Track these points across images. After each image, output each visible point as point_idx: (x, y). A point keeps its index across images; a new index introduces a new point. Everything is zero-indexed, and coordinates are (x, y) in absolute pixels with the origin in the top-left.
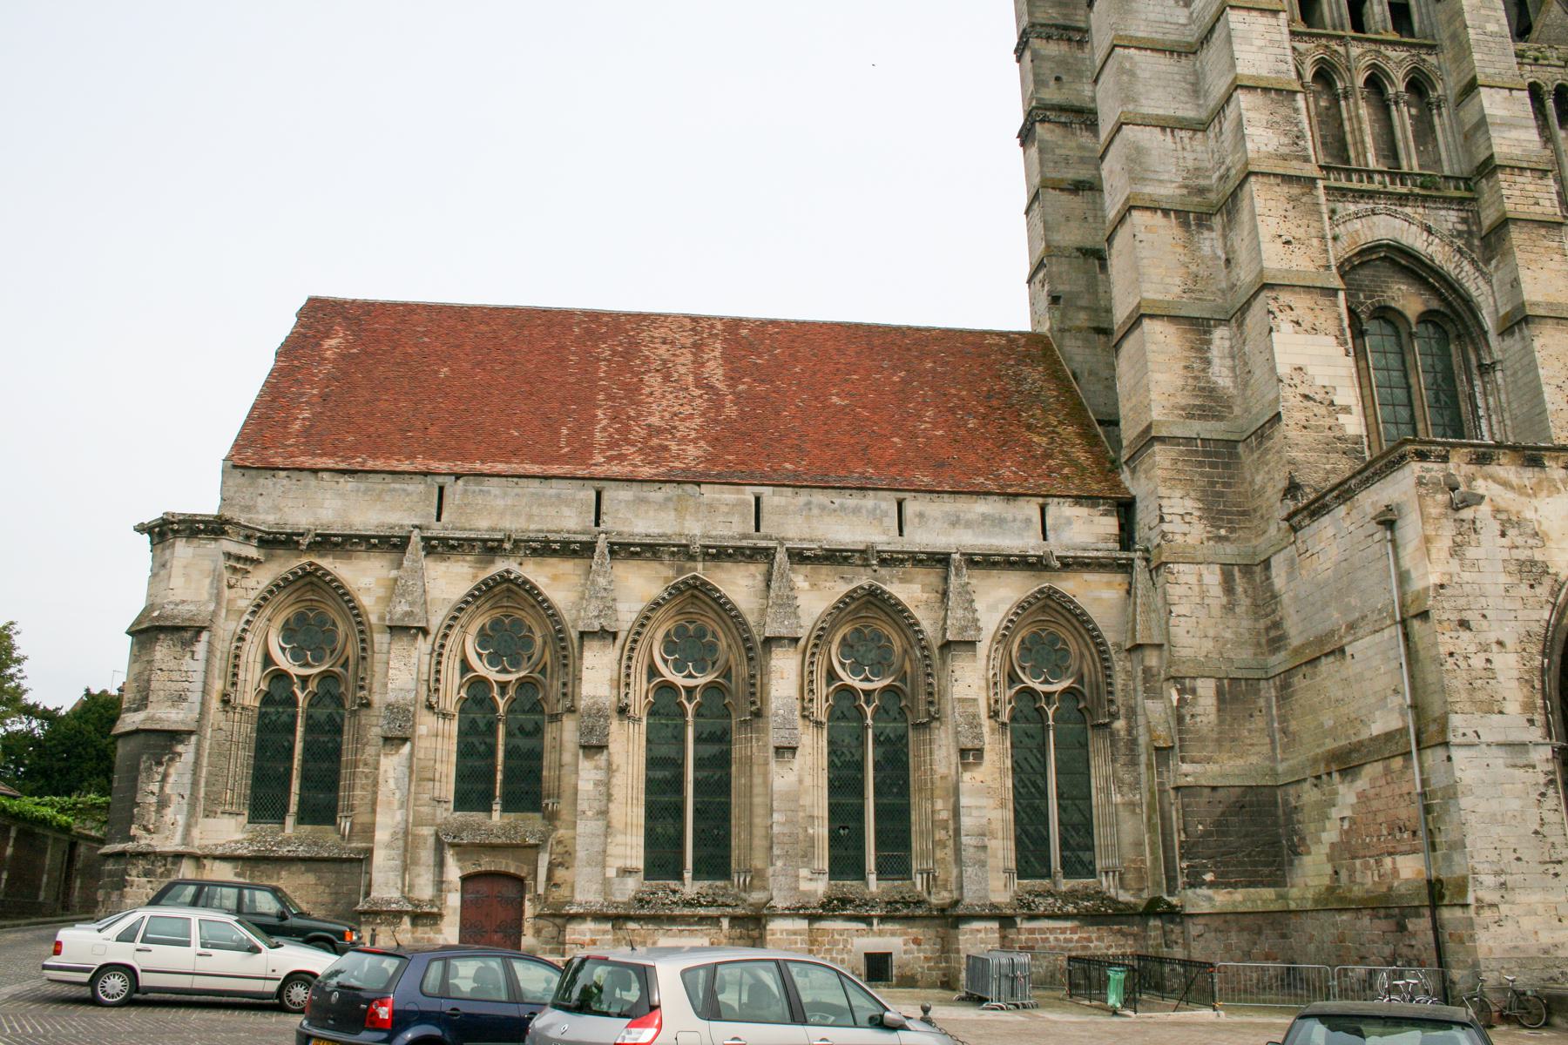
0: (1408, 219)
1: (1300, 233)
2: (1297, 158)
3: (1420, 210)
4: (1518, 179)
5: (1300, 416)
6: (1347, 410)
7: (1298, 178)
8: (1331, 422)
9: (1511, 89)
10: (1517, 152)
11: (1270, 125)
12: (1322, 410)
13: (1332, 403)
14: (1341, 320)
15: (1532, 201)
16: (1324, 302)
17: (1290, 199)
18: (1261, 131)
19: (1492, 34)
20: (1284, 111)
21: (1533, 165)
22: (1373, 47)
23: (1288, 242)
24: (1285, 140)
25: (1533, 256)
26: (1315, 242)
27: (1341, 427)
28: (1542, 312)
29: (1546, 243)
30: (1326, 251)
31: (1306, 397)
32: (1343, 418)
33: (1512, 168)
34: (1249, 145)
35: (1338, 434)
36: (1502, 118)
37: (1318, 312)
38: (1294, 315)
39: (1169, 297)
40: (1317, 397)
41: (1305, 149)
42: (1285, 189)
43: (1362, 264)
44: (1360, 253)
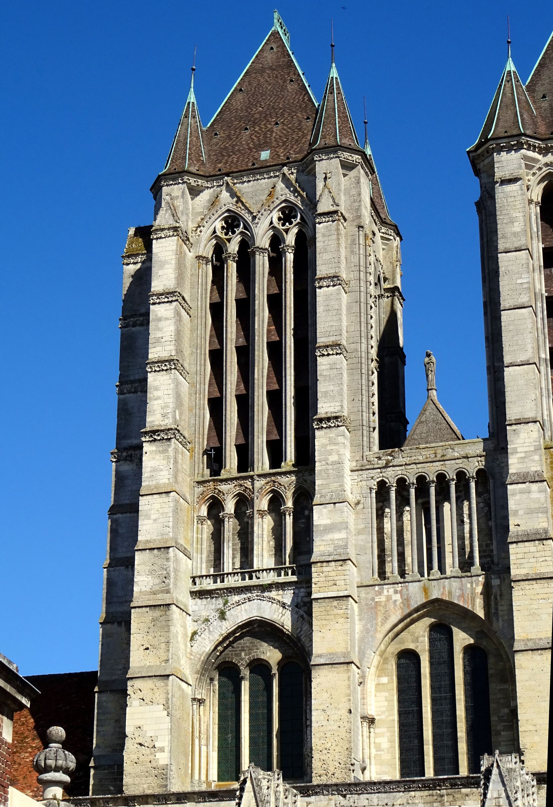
0: (271, 600)
1: (155, 642)
2: (162, 592)
3: (281, 592)
4: (325, 569)
5: (134, 757)
6: (162, 750)
7: (160, 605)
8: (151, 757)
9: (335, 503)
10: (331, 549)
11: (151, 573)
12: (148, 751)
13: (154, 747)
15: (331, 583)
18: (144, 578)
19: (334, 463)
20: (159, 562)
22: (273, 478)
23: (147, 649)
24: (157, 581)
25: (324, 622)
26: (163, 646)
27: (157, 761)
28: (322, 661)
29: (336, 611)
30: (168, 650)
31: (141, 745)
32: (159, 755)
33: (322, 562)
35: (154, 764)
36: (325, 525)
38: (140, 695)
39: (114, 678)
40: (146, 745)
41: (168, 585)
42: (151, 613)
44: (240, 627)
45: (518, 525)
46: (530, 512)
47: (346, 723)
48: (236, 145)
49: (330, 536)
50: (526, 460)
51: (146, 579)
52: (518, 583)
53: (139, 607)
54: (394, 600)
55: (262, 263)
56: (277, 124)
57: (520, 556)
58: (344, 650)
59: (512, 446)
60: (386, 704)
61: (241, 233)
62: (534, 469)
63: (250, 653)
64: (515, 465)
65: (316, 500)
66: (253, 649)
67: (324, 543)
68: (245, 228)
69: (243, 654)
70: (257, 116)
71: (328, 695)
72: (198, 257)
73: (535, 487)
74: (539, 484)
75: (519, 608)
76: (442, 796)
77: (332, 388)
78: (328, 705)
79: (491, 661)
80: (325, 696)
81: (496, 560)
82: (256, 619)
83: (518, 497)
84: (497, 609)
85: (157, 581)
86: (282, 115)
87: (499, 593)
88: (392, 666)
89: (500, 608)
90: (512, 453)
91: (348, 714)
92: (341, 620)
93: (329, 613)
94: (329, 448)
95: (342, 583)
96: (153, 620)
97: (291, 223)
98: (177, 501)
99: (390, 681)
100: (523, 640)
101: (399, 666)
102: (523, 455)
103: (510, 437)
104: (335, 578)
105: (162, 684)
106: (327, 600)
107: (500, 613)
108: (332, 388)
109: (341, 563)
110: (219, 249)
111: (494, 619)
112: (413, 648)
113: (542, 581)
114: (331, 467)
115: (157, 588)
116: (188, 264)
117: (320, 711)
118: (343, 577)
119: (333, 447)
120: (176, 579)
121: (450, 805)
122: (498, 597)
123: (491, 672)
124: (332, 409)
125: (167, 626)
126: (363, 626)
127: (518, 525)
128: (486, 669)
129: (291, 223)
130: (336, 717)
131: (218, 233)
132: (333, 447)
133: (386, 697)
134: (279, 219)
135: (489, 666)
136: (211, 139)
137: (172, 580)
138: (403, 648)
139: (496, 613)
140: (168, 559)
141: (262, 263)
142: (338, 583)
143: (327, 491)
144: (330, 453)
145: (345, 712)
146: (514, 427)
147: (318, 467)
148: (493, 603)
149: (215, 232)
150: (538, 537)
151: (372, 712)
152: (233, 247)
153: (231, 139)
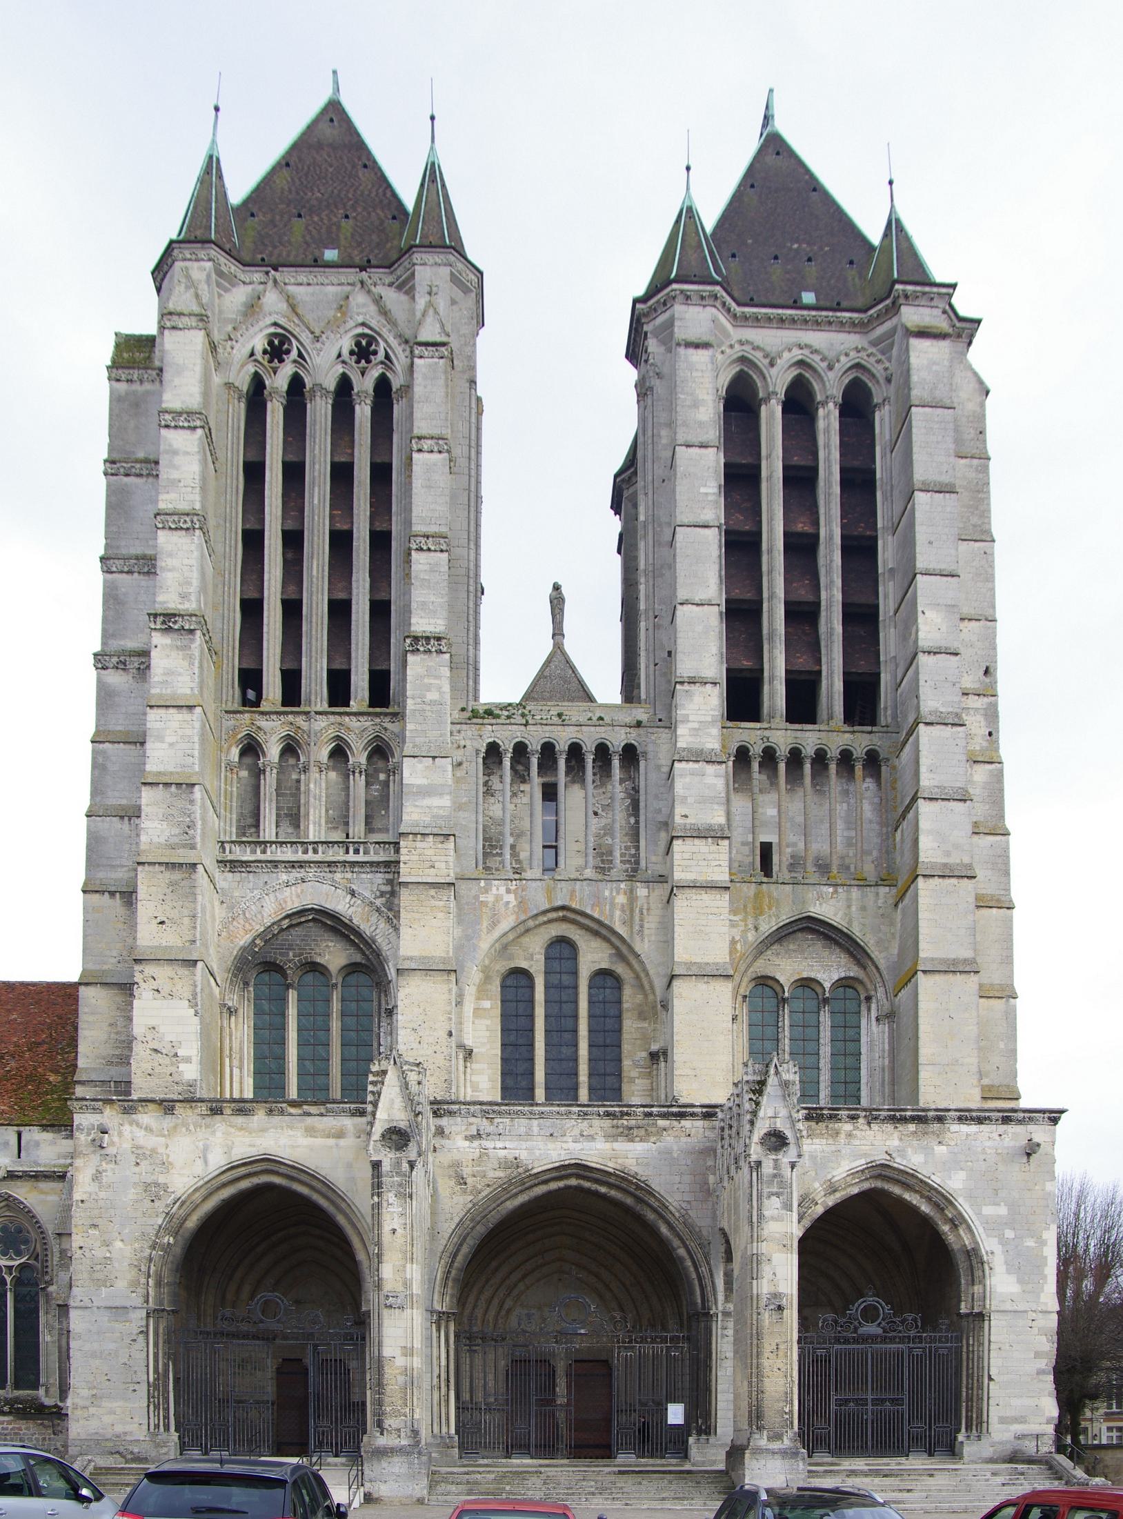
1: (174, 914)
2: (184, 846)
4: (419, 844)
7: (181, 865)
9: (434, 758)
10: (427, 819)
14: (196, 986)
16: (183, 971)
17: (172, 884)
18: (156, 824)
19: (432, 703)
20: (180, 804)
21: (436, 831)
25: (416, 916)
26: (186, 921)
29: (433, 903)
30: (195, 928)
34: (143, 838)
36: (418, 786)
37: (176, 980)
45: (686, 816)
46: (703, 800)
47: (444, 1048)
48: (285, 234)
49: (427, 802)
50: (700, 733)
52: (681, 890)
53: (150, 864)
54: (502, 899)
55: (320, 412)
56: (347, 217)
57: (686, 856)
59: (683, 712)
60: (488, 1034)
61: (295, 361)
62: (709, 746)
64: (685, 737)
65: (408, 749)
67: (419, 810)
68: (300, 355)
70: (315, 203)
72: (229, 386)
73: (710, 769)
74: (717, 767)
75: (681, 922)
76: (631, 1128)
77: (433, 598)
79: (627, 992)
81: (643, 864)
83: (687, 780)
84: (642, 926)
85: (177, 831)
86: (354, 208)
87: (645, 907)
89: (646, 925)
90: (683, 722)
92: (440, 915)
94: (426, 681)
95: (443, 865)
97: (368, 361)
98: (203, 726)
99: (492, 1005)
100: (686, 964)
101: (504, 987)
102: (696, 725)
103: (679, 698)
104: (434, 858)
106: (421, 887)
107: (646, 932)
108: (433, 598)
109: (442, 838)
110: (258, 384)
111: (637, 938)
113: (714, 891)
114: (428, 708)
116: (214, 392)
118: (443, 858)
119: (432, 681)
120: (203, 834)
121: (641, 1141)
122: (645, 912)
123: (625, 1006)
124: (432, 629)
125: (192, 895)
127: (686, 816)
128: (620, 1002)
129: (368, 361)
130: (431, 1040)
131: (259, 356)
132: (432, 681)
134: (352, 353)
135: (625, 998)
136: (245, 220)
137: (199, 831)
139: (641, 931)
140: (192, 802)
141: (320, 412)
142: (436, 865)
143: (422, 739)
144: (428, 688)
146: (686, 687)
147: (410, 703)
148: (637, 918)
149: (252, 354)
150: (712, 834)
151: (469, 1042)
152: (279, 381)
153: (275, 226)
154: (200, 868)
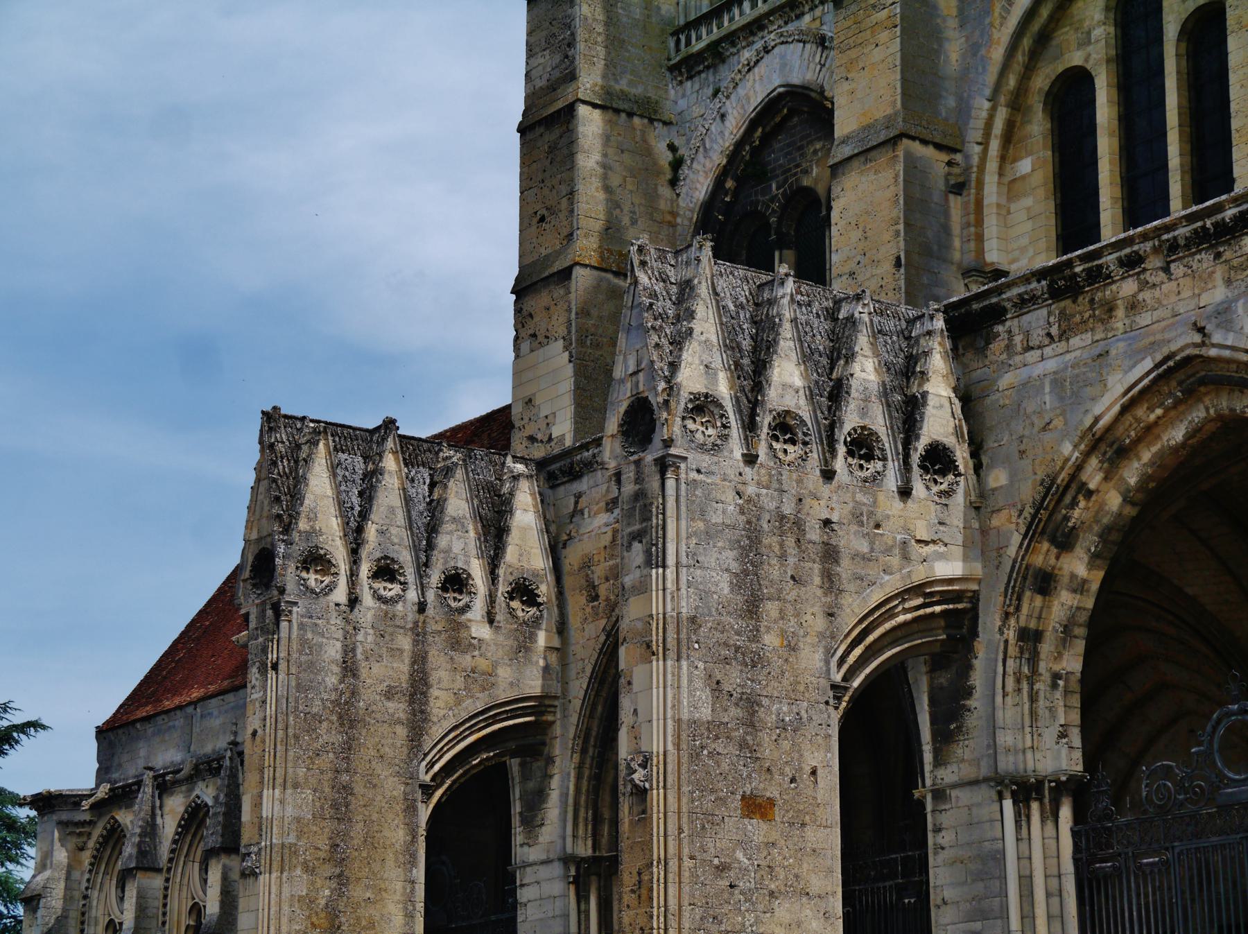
25: (853, 54)
43: (765, 139)
44: (753, 124)
51: (542, 60)
58: (889, 111)
63: (786, 180)
66: (790, 170)
69: (774, 186)
71: (859, 233)
78: (859, 258)
80: (855, 235)
82: (780, 94)
88: (1038, 126)
91: (894, 271)
93: (863, 26)
96: (552, 149)
105: (562, 292)
112: (1080, 63)
115: (557, 74)
117: (845, 277)
126: (967, 38)
133: (1028, 209)
138: (1060, 70)
145: (887, 266)
154: (583, 110)
